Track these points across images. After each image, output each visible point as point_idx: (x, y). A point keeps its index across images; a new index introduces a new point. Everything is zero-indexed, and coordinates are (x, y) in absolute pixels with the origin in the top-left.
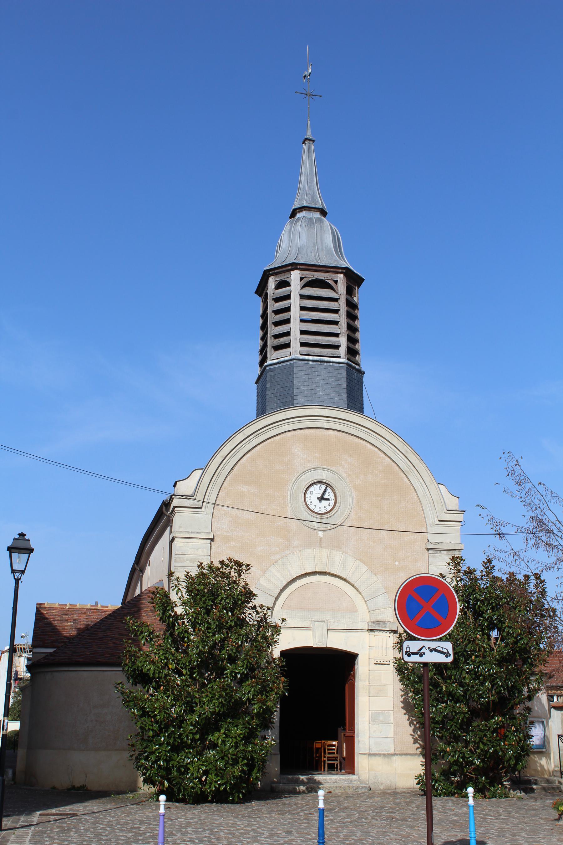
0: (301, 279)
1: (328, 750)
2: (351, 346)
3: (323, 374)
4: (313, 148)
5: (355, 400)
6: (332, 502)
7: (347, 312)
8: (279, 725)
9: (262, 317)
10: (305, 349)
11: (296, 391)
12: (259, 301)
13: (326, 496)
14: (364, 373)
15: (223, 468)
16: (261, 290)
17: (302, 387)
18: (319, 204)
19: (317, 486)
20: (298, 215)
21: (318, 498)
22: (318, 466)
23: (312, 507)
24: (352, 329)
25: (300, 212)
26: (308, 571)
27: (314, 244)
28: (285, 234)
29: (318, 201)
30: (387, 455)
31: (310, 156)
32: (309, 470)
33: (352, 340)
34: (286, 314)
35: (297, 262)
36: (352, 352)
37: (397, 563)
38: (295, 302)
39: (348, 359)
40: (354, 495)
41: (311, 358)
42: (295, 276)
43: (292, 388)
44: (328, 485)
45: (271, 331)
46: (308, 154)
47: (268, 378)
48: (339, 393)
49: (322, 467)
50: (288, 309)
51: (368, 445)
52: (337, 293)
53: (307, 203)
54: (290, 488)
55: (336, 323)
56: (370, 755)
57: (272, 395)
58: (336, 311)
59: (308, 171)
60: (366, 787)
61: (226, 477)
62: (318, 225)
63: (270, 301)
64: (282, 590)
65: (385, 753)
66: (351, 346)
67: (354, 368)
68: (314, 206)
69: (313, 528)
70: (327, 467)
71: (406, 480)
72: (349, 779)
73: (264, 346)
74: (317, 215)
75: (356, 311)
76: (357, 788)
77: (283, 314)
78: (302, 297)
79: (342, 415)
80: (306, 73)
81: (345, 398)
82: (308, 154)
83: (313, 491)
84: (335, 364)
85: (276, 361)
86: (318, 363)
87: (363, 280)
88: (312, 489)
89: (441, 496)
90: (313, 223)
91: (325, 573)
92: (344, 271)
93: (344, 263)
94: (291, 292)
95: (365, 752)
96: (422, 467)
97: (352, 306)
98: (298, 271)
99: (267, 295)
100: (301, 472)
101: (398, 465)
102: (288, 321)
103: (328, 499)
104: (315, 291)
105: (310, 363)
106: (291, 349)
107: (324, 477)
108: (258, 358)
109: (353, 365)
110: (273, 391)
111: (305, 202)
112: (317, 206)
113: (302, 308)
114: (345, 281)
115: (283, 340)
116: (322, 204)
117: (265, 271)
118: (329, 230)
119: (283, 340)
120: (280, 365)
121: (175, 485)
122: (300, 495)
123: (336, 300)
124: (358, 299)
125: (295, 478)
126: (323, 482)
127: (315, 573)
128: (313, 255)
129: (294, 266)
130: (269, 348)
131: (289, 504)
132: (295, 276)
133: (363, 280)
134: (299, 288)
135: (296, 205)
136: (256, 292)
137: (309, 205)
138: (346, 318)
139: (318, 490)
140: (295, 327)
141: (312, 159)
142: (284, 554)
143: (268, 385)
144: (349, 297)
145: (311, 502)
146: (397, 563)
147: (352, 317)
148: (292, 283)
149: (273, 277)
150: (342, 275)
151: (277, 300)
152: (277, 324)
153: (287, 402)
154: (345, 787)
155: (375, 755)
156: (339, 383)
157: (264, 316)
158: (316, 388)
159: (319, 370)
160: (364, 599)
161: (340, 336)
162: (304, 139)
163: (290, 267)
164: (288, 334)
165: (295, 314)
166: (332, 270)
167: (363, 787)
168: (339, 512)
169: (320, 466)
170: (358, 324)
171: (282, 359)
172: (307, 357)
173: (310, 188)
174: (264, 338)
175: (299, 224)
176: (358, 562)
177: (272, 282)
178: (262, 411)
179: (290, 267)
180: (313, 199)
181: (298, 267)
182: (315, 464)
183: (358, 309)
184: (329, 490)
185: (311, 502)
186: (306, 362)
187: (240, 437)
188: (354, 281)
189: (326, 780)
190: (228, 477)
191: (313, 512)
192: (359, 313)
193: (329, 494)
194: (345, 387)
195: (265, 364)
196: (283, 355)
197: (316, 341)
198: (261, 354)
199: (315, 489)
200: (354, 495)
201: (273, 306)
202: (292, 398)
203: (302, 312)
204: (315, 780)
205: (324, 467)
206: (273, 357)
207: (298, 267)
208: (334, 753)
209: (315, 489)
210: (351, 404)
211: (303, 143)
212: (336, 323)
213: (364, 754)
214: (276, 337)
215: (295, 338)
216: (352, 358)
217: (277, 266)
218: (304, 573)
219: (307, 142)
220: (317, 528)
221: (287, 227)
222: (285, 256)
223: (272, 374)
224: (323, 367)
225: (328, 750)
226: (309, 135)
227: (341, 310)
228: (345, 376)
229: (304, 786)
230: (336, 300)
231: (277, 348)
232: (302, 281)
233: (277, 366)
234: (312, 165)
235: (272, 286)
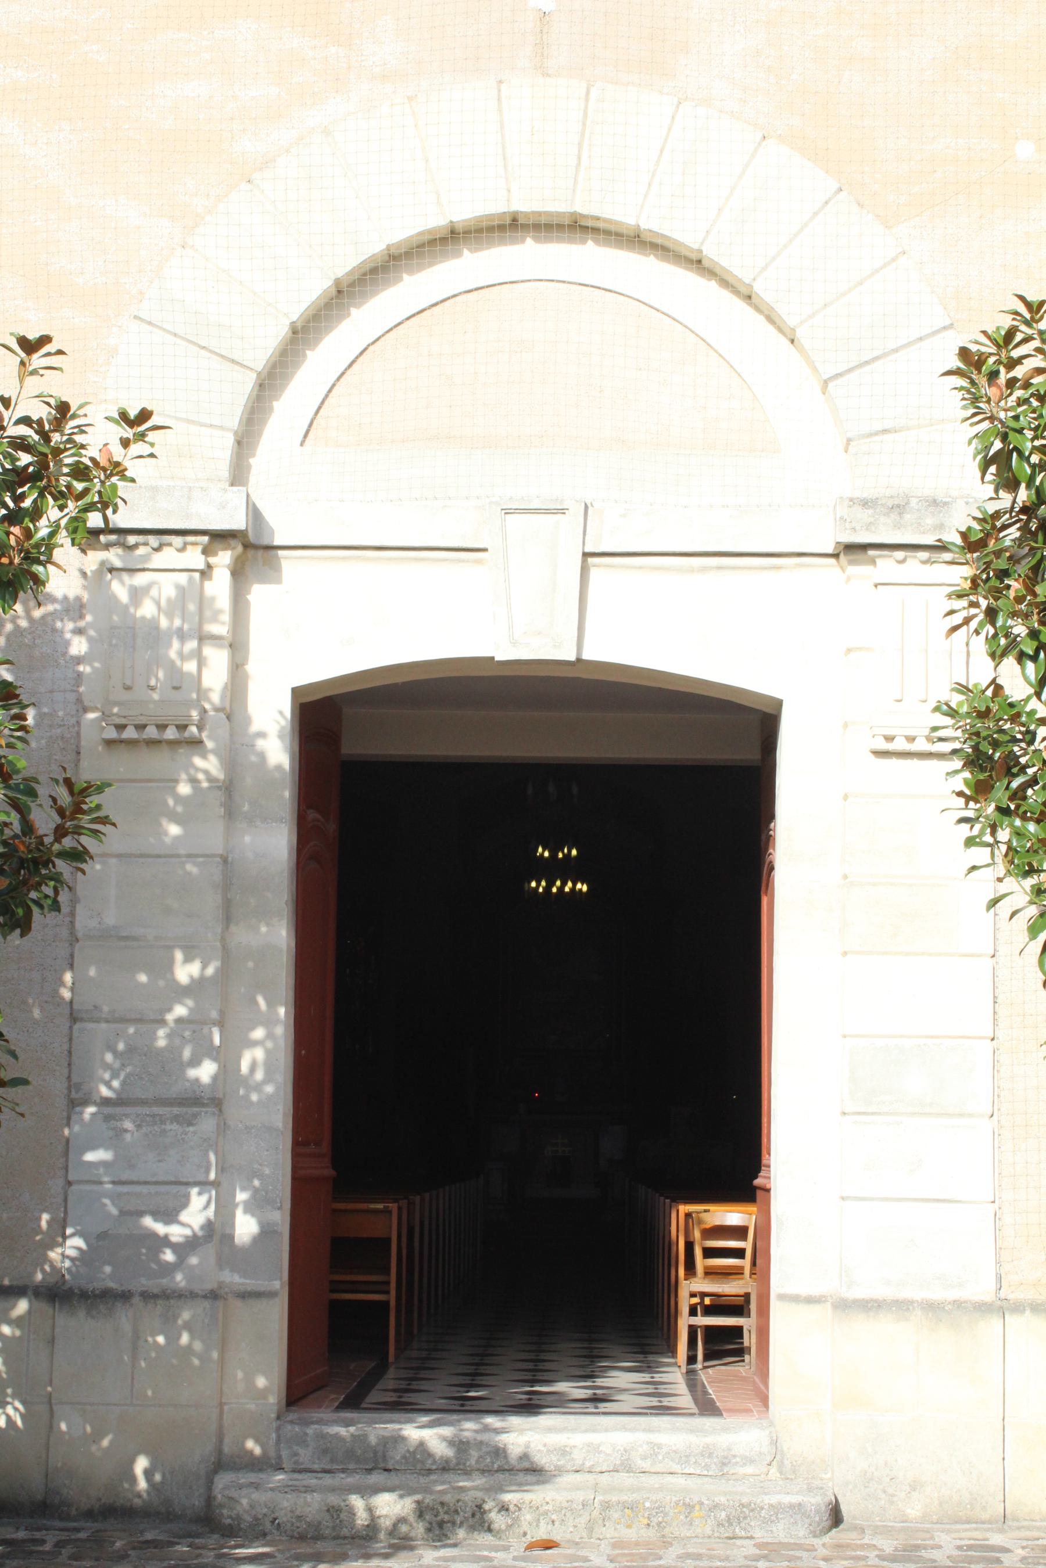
1: (709, 1253)
8: (278, 1115)
26: (464, 210)
56: (844, 1306)
60: (797, 1508)
64: (304, 334)
65: (938, 1294)
72: (708, 1452)
76: (742, 1513)
91: (575, 227)
95: (815, 1291)
127: (511, 227)
146: (1025, 150)
154: (659, 1509)
155: (870, 1306)
160: (815, 369)
167: (777, 1509)
189: (563, 1451)
204: (499, 1452)
208: (737, 1272)
213: (810, 1300)
218: (435, 220)
225: (709, 1253)
229: (405, 1490)
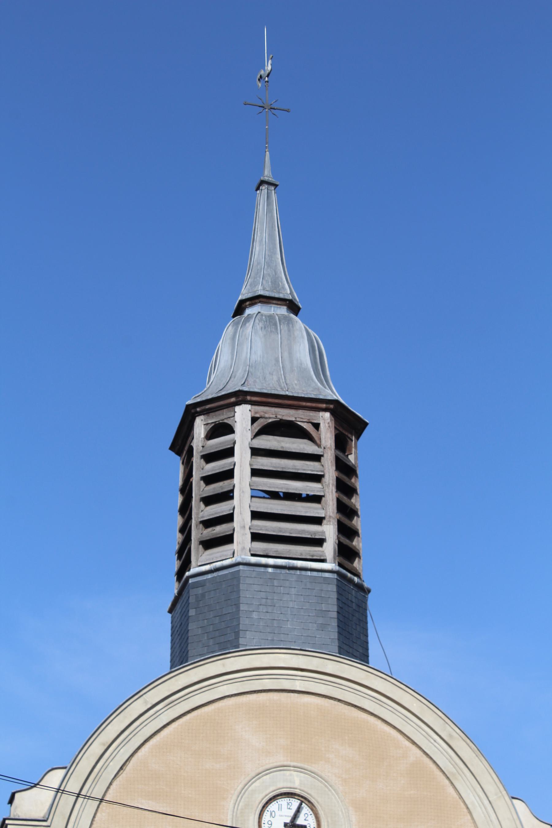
0: (254, 420)
2: (345, 541)
3: (293, 591)
4: (274, 197)
5: (353, 641)
7: (338, 480)
9: (182, 491)
10: (261, 546)
11: (244, 622)
12: (177, 465)
14: (369, 591)
15: (105, 767)
16: (181, 444)
17: (255, 615)
18: (286, 292)
19: (284, 802)
20: (248, 311)
22: (285, 763)
24: (346, 511)
25: (252, 305)
27: (277, 360)
28: (224, 347)
29: (283, 288)
30: (414, 743)
31: (270, 211)
32: (268, 771)
33: (347, 531)
34: (227, 482)
35: (245, 389)
36: (347, 553)
38: (242, 462)
39: (340, 565)
41: (271, 561)
42: (242, 415)
43: (236, 616)
44: (303, 799)
45: (197, 514)
46: (266, 211)
47: (192, 600)
48: (322, 627)
49: (292, 764)
50: (229, 474)
51: (379, 723)
52: (319, 446)
53: (264, 289)
55: (317, 499)
57: (200, 631)
58: (317, 478)
59: (265, 235)
61: (111, 784)
62: (284, 328)
63: (197, 460)
66: (345, 541)
67: (351, 581)
68: (277, 296)
71: (451, 790)
73: (187, 541)
74: (283, 310)
75: (353, 480)
77: (221, 484)
78: (256, 452)
79: (331, 666)
80: (262, 72)
81: (335, 635)
82: (266, 211)
83: (276, 810)
84: (315, 574)
85: (207, 568)
86: (284, 571)
87: (366, 424)
88: (273, 806)
89: (518, 822)
90: (275, 324)
92: (332, 406)
93: (331, 393)
94: (234, 443)
96: (479, 766)
97: (345, 469)
98: (248, 407)
99: (191, 449)
100: (253, 774)
101: (434, 762)
102: (228, 496)
104: (278, 441)
105: (270, 570)
106: (235, 546)
107: (297, 784)
108: (176, 565)
109: (349, 575)
110: (201, 623)
111: (260, 287)
112: (281, 296)
113: (256, 473)
114: (332, 425)
115: (220, 530)
116: (291, 293)
117: (188, 406)
118: (303, 337)
119: (220, 530)
120: (215, 574)
121: (11, 801)
123: (316, 458)
124: (356, 458)
128: (275, 378)
129: (241, 397)
130: (194, 544)
132: (242, 415)
133: (366, 424)
134: (249, 435)
135: (245, 294)
136: (172, 448)
137: (267, 294)
138: (334, 490)
140: (242, 505)
141: (272, 217)
143: (192, 612)
144: (341, 455)
147: (345, 489)
148: (238, 428)
149: (202, 417)
150: (327, 415)
151: (209, 458)
152: (208, 501)
153: (227, 641)
156: (324, 607)
157: (186, 489)
158: (282, 617)
159: (287, 584)
161: (325, 522)
162: (258, 182)
163: (233, 400)
164: (229, 518)
165: (242, 482)
166: (309, 404)
170: (356, 502)
171: (218, 564)
172: (264, 560)
173: (269, 266)
174: (185, 529)
175: (250, 325)
177: (200, 428)
178: (180, 657)
179: (233, 400)
180: (275, 282)
181: (249, 398)
182: (281, 759)
183: (357, 476)
184: (306, 809)
186: (262, 569)
187: (138, 707)
188: (349, 425)
190: (114, 784)
192: (359, 483)
194: (335, 615)
195: (187, 574)
196: (220, 556)
197: (280, 530)
198: (179, 558)
199: (280, 808)
201: (201, 468)
202: (237, 637)
203: (256, 479)
206: (202, 561)
207: (249, 398)
209: (280, 808)
210: (346, 647)
211: (258, 189)
212: (317, 499)
214: (208, 523)
215: (242, 526)
216: (346, 563)
217: (210, 397)
219: (264, 187)
221: (229, 330)
222: (224, 381)
223: (200, 591)
224: (294, 578)
226: (267, 175)
227: (327, 476)
228: (334, 596)
230: (316, 458)
231: (209, 544)
232: (255, 424)
233: (209, 576)
234: (273, 227)
235: (200, 434)
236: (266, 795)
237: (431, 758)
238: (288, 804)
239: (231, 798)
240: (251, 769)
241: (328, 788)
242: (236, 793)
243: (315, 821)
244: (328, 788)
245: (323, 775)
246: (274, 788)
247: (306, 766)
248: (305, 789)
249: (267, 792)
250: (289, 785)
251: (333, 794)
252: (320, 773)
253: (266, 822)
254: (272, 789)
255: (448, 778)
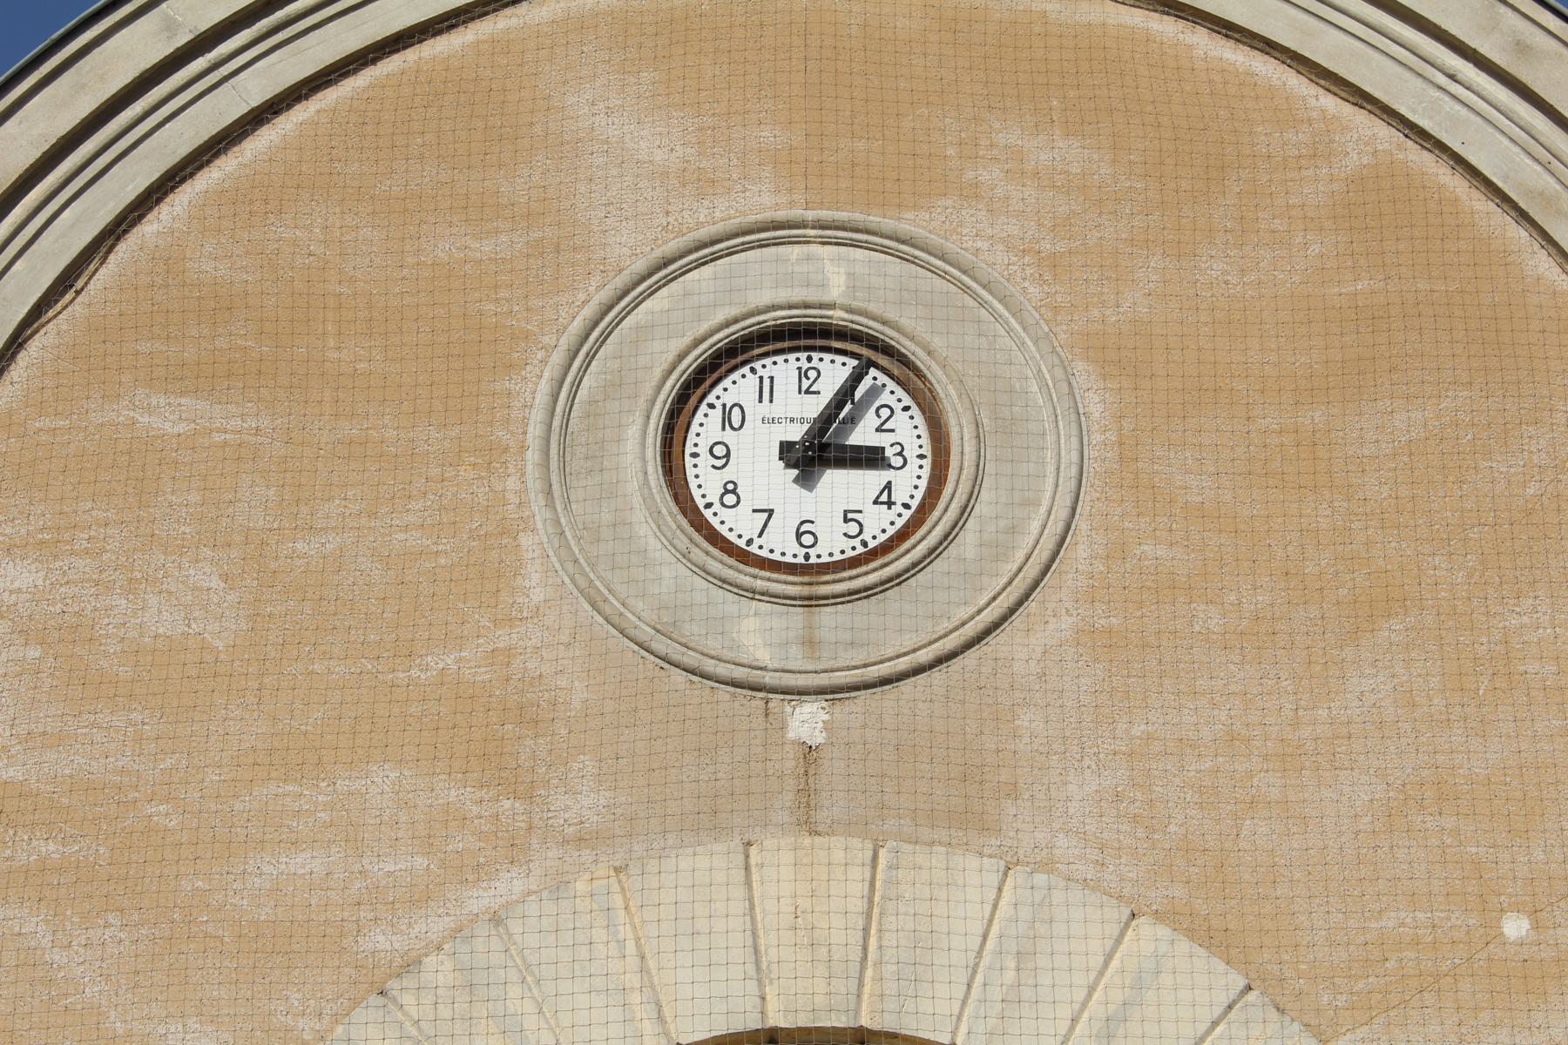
6: (909, 483)
13: (863, 435)
19: (783, 369)
21: (786, 449)
22: (781, 215)
23: (737, 524)
32: (708, 250)
37: (1515, 927)
40: (1094, 405)
44: (870, 349)
49: (810, 215)
54: (544, 387)
69: (739, 673)
70: (858, 217)
100: (640, 266)
101: (1459, 161)
103: (871, 458)
107: (836, 289)
122: (633, 432)
125: (588, 312)
126: (842, 334)
131: (537, 503)
139: (788, 394)
142: (480, 900)
145: (731, 489)
146: (1515, 927)
168: (968, 539)
169: (796, 213)
176: (1149, 936)
182: (763, 202)
185: (731, 489)
191: (743, 556)
193: (890, 423)
199: (766, 391)
200: (1094, 405)
205: (825, 214)
209: (766, 391)
220: (769, 679)
236: (698, 342)
237: (1441, 147)
238: (802, 374)
239: (544, 362)
240: (630, 248)
241: (975, 296)
242: (565, 342)
243: (923, 430)
244: (975, 296)
245: (951, 247)
246: (735, 311)
247: (874, 220)
248: (872, 308)
249: (704, 327)
250: (798, 295)
251: (997, 317)
252: (935, 240)
253: (703, 450)
254: (721, 316)
255: (1523, 216)
